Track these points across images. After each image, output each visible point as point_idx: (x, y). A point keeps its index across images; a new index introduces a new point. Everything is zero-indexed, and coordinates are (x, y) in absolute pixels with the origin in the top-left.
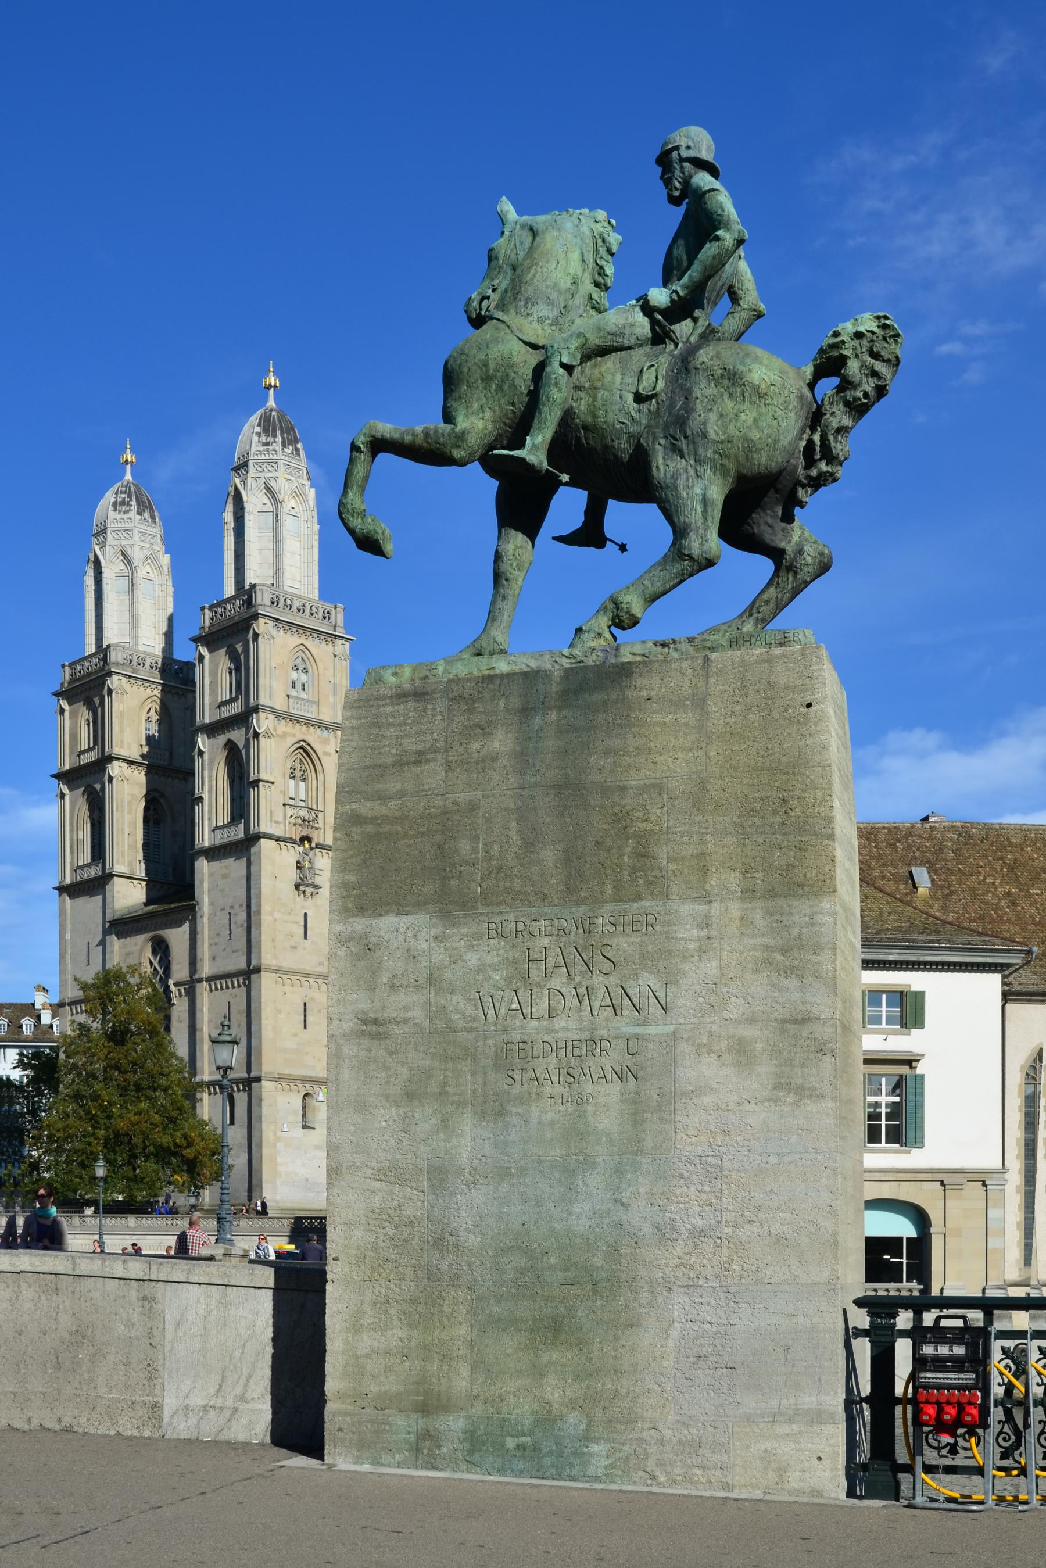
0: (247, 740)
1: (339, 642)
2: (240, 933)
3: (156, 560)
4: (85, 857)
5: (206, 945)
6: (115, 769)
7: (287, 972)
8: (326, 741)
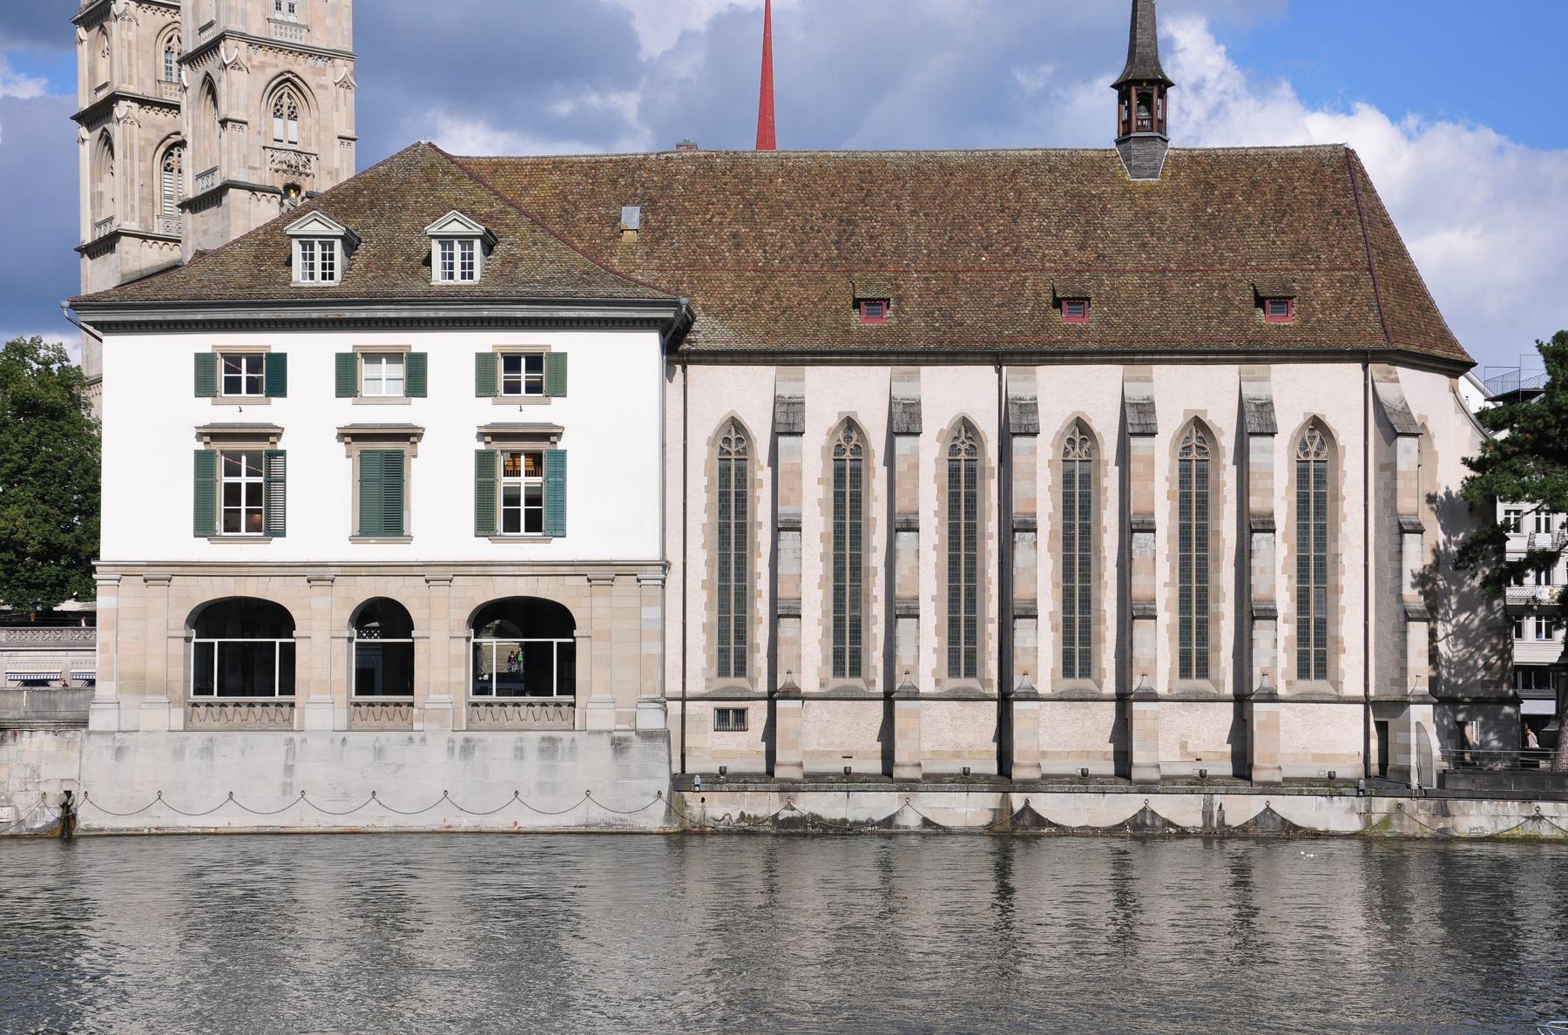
8: (322, 72)
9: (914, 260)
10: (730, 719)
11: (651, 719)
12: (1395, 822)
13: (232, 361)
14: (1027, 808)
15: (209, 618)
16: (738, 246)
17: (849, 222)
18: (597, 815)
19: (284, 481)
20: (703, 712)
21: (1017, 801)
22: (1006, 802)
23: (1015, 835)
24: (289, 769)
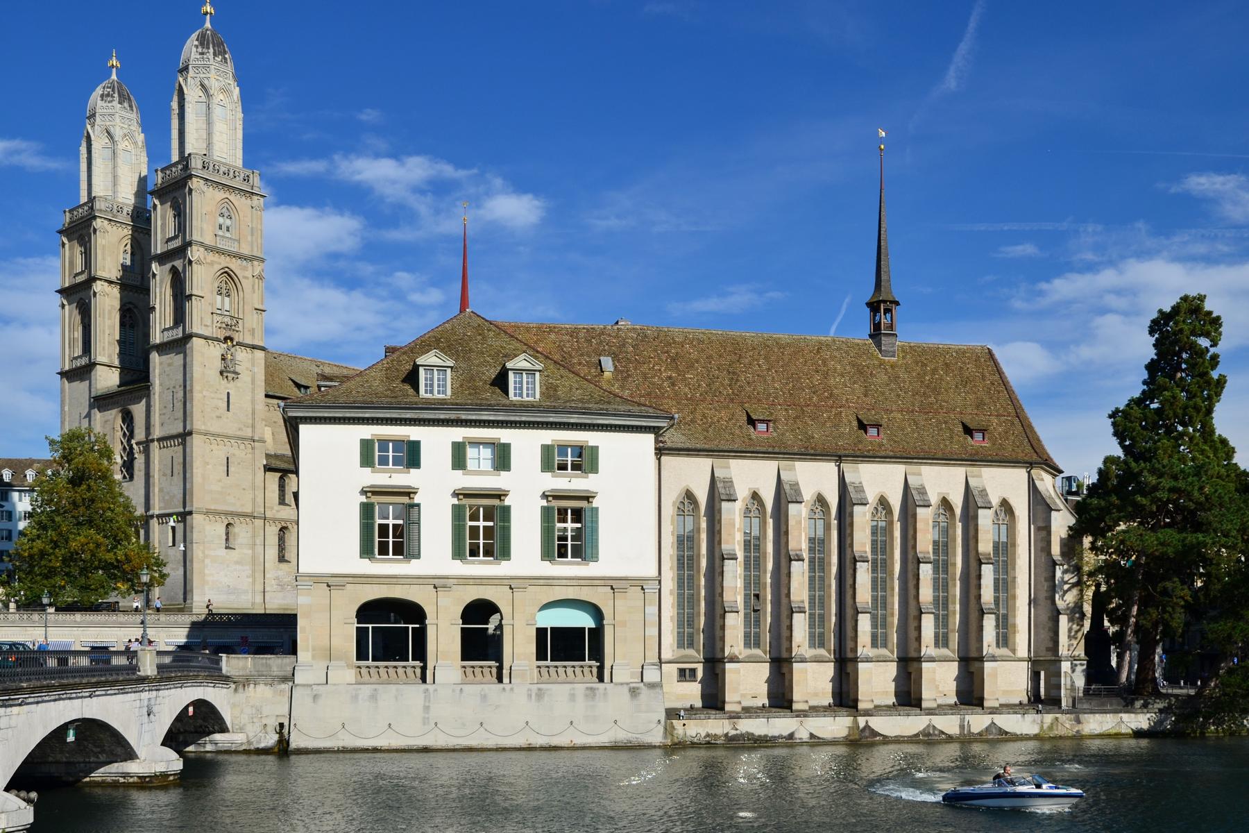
0: (184, 266)
1: (255, 198)
2: (179, 405)
3: (132, 137)
4: (78, 351)
5: (157, 415)
6: (98, 287)
7: (213, 435)
8: (245, 269)
9: (776, 398)
10: (684, 675)
11: (651, 675)
13: (384, 443)
14: (867, 726)
15: (368, 611)
16: (673, 384)
17: (734, 373)
18: (621, 736)
19: (419, 524)
20: (671, 670)
21: (862, 721)
22: (856, 722)
23: (862, 741)
24: (427, 708)
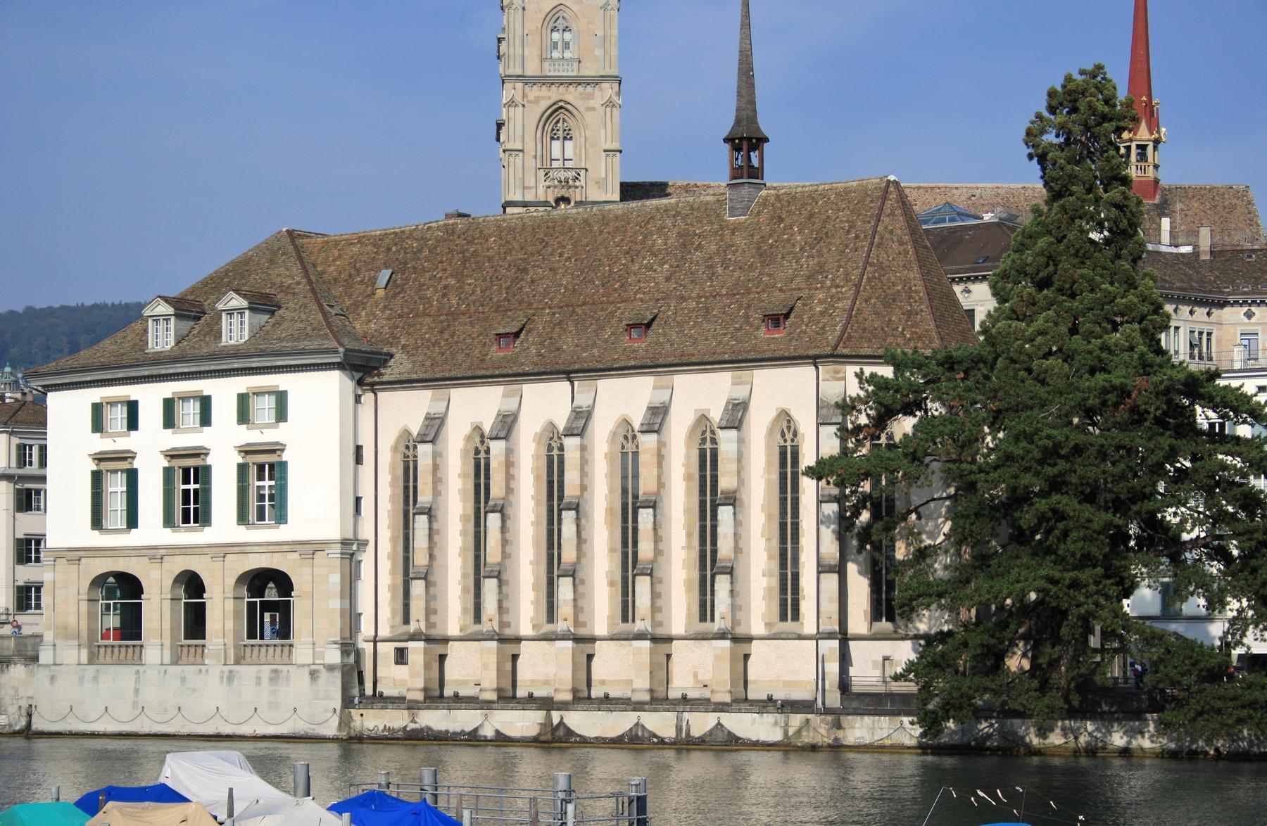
8: (590, 96)
12: (804, 733)
14: (561, 723)
21: (556, 716)
22: (549, 718)
24: (137, 691)
